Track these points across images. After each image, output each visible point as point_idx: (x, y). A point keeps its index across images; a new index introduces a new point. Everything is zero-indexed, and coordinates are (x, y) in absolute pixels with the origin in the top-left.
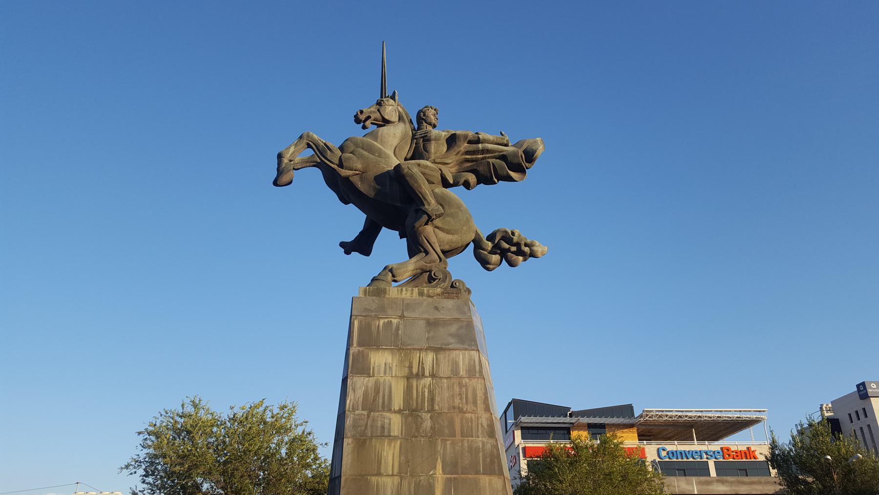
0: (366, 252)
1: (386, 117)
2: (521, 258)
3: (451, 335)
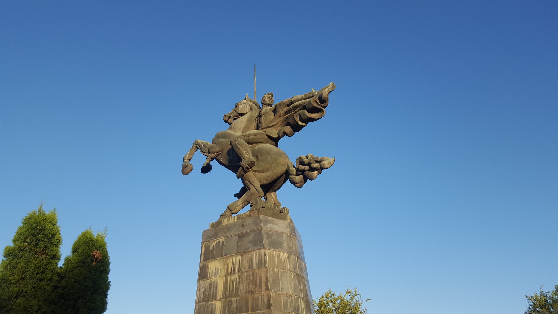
1: (240, 112)
2: (316, 173)
3: (250, 242)
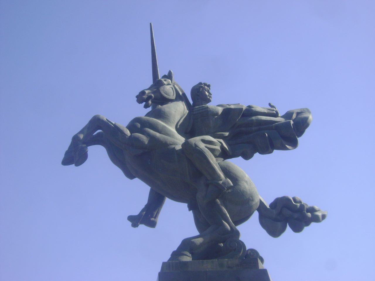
0: (152, 224)
